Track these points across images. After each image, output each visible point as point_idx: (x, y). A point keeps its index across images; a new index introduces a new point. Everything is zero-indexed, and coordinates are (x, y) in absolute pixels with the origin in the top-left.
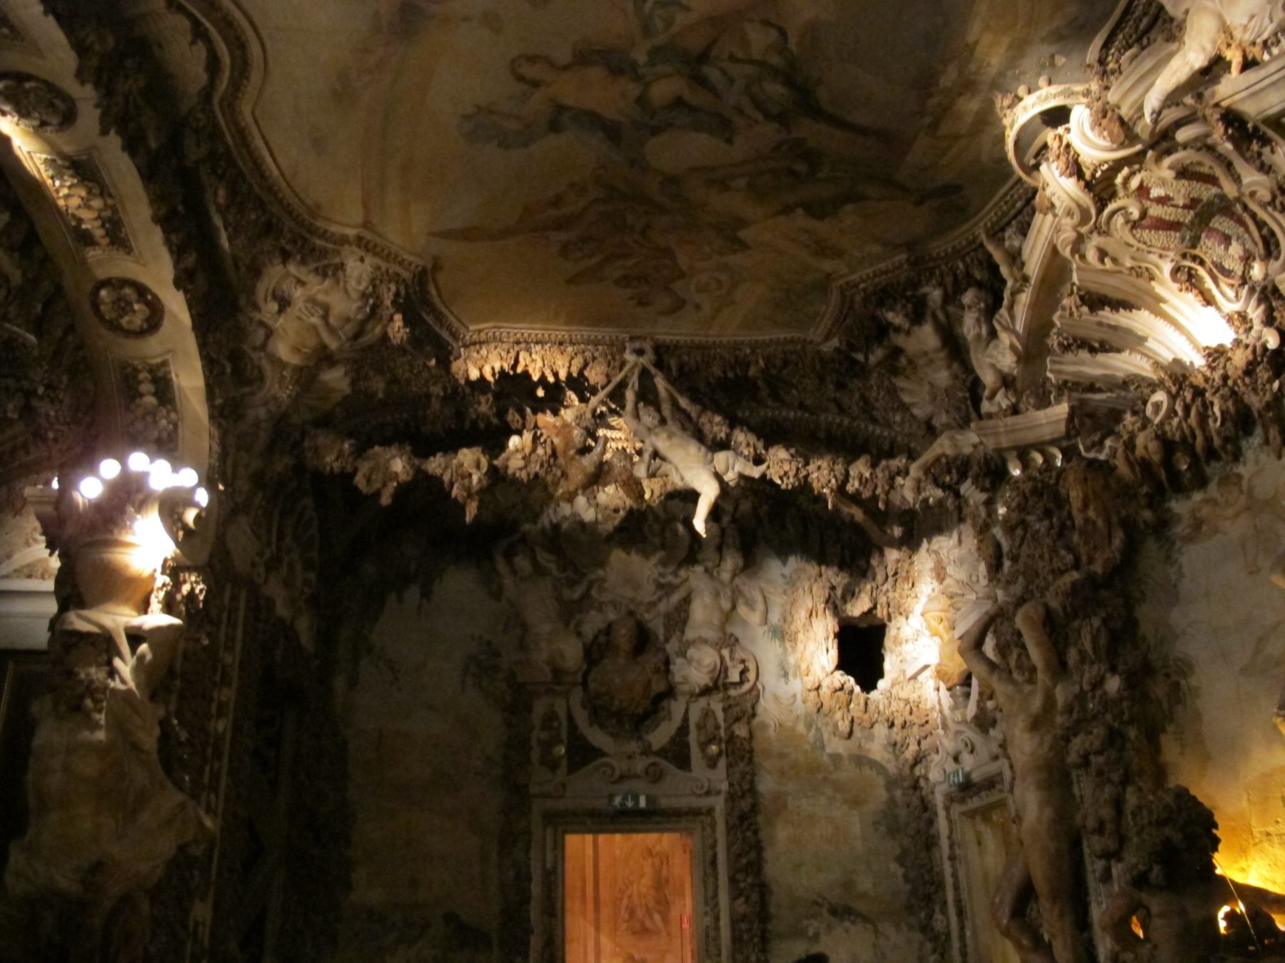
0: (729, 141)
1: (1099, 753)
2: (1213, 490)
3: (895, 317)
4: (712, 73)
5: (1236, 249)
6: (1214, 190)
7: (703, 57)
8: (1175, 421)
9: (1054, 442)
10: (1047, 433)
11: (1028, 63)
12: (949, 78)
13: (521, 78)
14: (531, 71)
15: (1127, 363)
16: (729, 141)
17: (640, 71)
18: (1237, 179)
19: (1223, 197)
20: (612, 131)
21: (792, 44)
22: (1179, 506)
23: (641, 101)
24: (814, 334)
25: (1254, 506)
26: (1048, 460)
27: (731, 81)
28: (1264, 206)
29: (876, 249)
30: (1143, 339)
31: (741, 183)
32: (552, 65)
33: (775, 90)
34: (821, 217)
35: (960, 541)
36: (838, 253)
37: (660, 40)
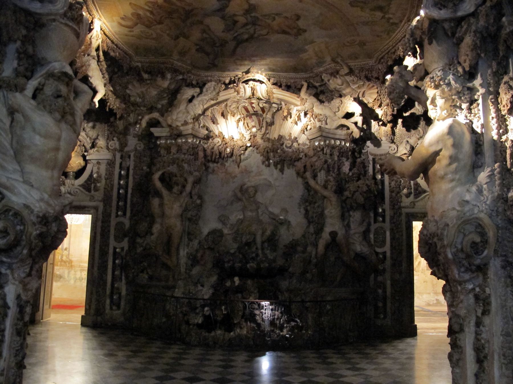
1: (194, 216)
2: (219, 164)
3: (169, 76)
5: (253, 124)
6: (261, 113)
8: (220, 147)
9: (199, 138)
10: (201, 135)
11: (263, 67)
15: (212, 127)
18: (267, 114)
19: (261, 116)
22: (211, 165)
24: (136, 58)
25: (227, 172)
26: (197, 141)
28: (267, 123)
29: (189, 62)
30: (218, 124)
35: (94, 127)
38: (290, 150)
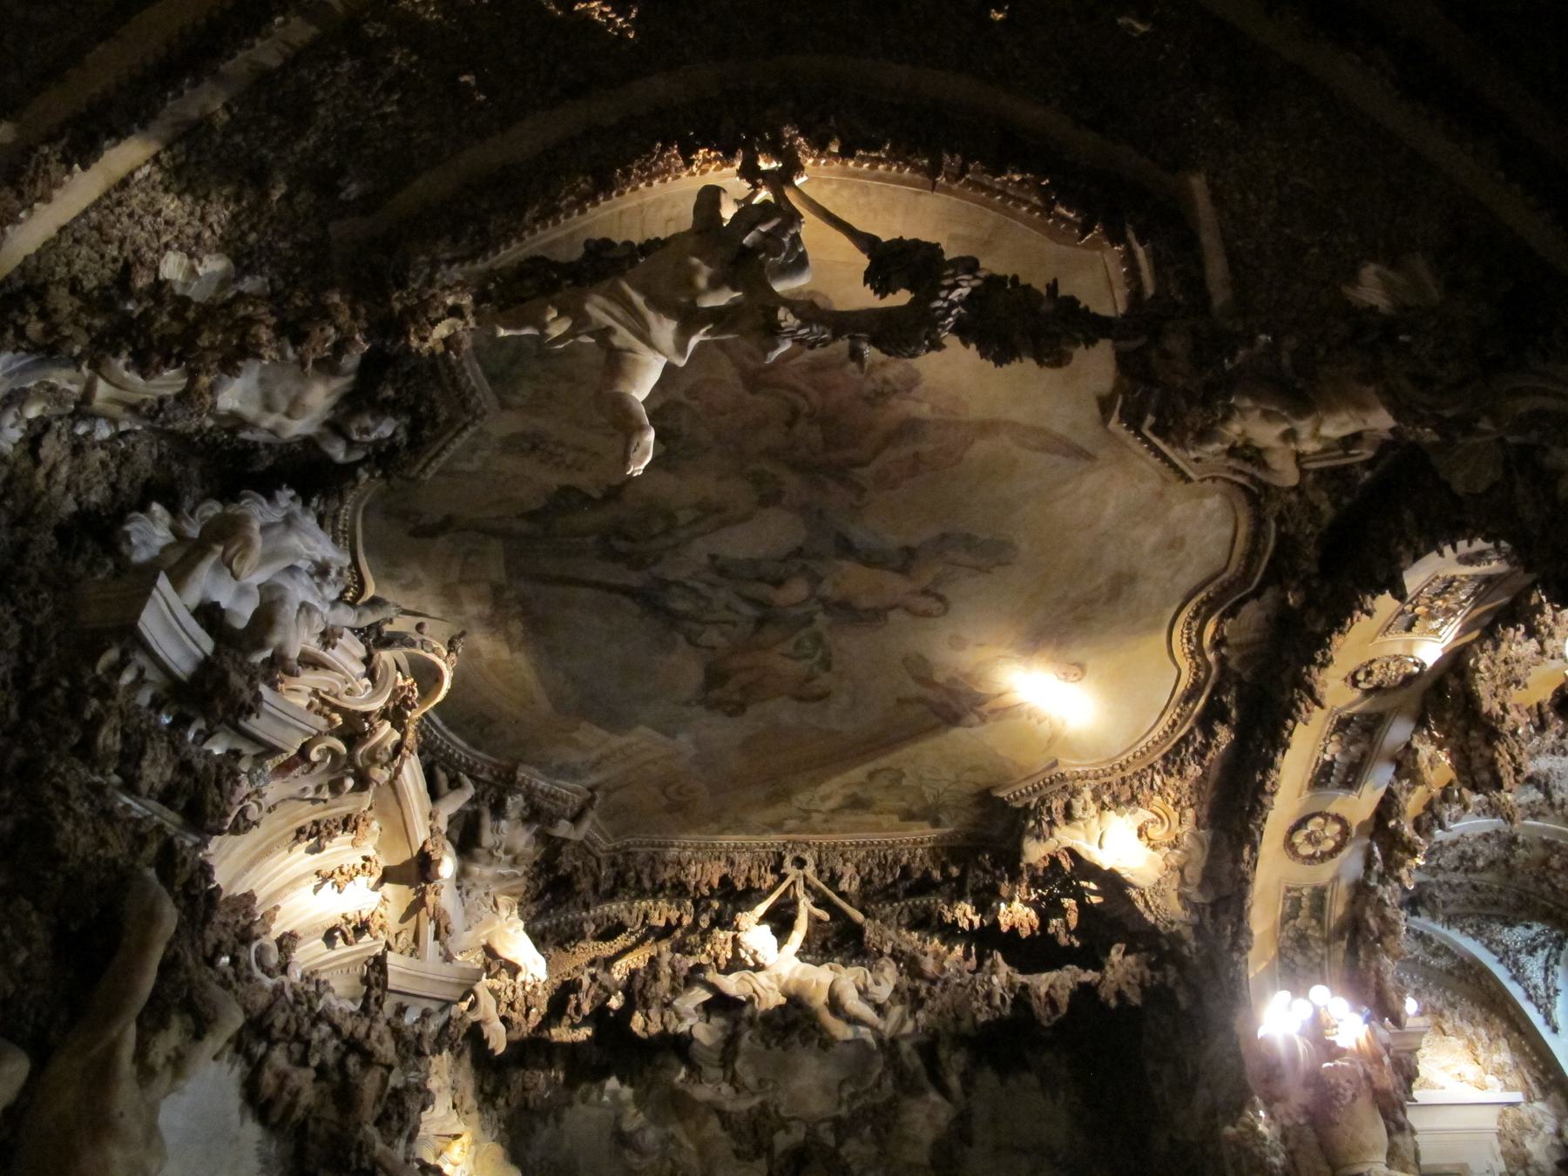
0: (713, 557)
4: (748, 611)
7: (761, 622)
12: (516, 628)
13: (941, 598)
14: (933, 605)
16: (713, 557)
17: (820, 606)
20: (846, 548)
21: (681, 638)
23: (817, 580)
27: (728, 607)
31: (683, 517)
32: (907, 609)
33: (682, 605)
34: (566, 490)
36: (510, 444)
37: (803, 633)
38: (268, 982)
